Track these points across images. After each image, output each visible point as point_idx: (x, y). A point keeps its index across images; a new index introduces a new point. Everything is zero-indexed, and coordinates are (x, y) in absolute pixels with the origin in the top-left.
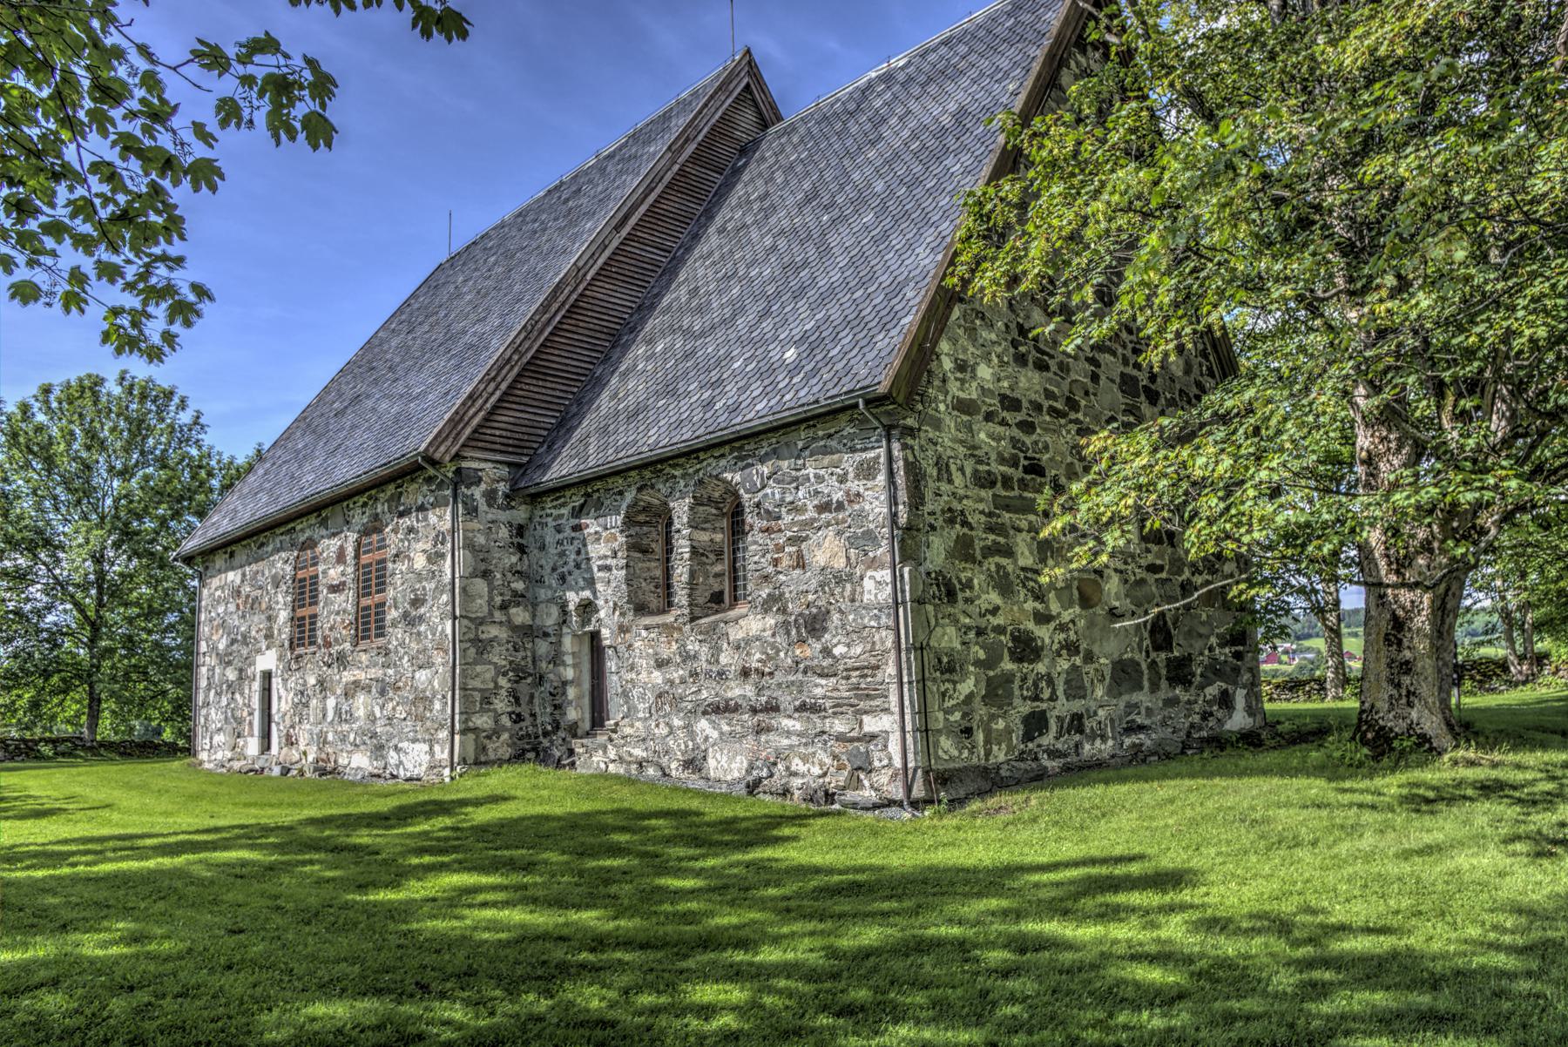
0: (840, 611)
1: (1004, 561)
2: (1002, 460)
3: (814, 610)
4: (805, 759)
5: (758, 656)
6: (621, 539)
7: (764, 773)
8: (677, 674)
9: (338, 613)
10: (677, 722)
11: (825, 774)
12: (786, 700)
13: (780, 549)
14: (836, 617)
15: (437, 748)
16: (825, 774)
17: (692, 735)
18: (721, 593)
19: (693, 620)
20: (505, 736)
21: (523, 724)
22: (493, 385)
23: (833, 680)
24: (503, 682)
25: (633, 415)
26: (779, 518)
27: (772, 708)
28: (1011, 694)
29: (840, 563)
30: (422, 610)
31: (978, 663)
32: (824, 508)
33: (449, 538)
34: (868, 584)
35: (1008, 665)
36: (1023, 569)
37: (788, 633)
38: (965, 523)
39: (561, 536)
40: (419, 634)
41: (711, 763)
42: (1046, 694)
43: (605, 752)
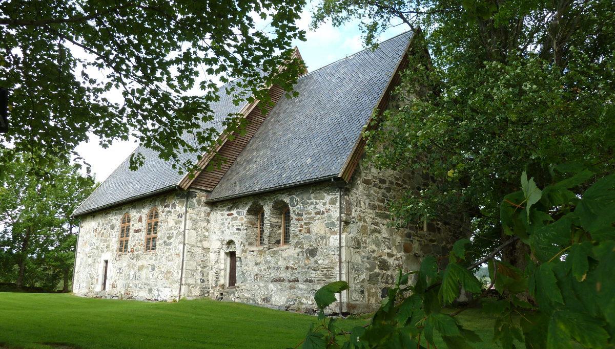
0: (322, 248)
1: (378, 235)
2: (379, 201)
3: (313, 248)
4: (306, 298)
5: (292, 262)
6: (245, 220)
7: (292, 303)
10: (261, 285)
11: (313, 304)
12: (301, 278)
13: (301, 226)
14: (320, 250)
15: (174, 290)
16: (313, 304)
18: (280, 241)
19: (269, 249)
20: (199, 287)
21: (205, 284)
22: (203, 163)
23: (318, 272)
24: (199, 268)
25: (252, 177)
26: (302, 216)
27: (296, 281)
28: (378, 281)
29: (322, 233)
30: (171, 241)
31: (367, 269)
32: (318, 213)
33: (184, 216)
34: (331, 239)
35: (377, 270)
36: (384, 238)
37: (303, 255)
38: (365, 221)
39: (223, 217)
40: (170, 249)
41: (273, 299)
42: (391, 281)
43: (234, 295)
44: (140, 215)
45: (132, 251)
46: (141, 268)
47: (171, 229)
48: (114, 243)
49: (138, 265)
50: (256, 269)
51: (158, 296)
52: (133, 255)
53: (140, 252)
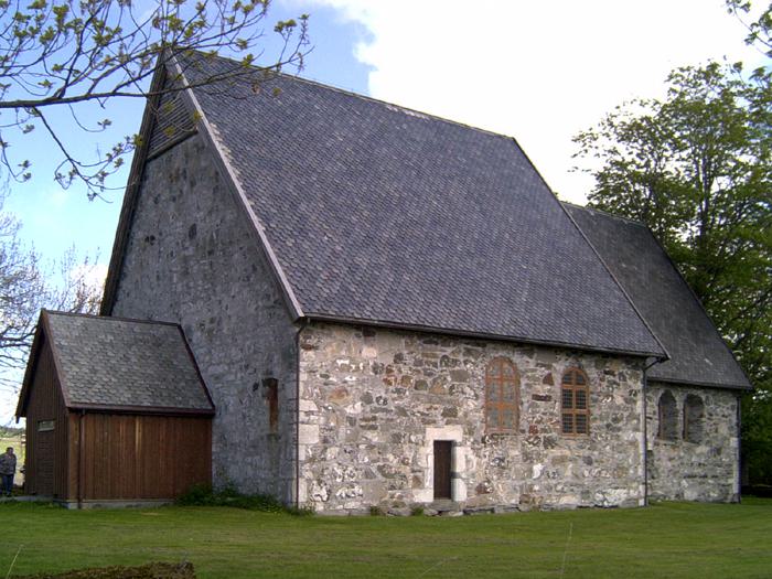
8: (676, 463)
9: (544, 414)
17: (680, 484)
27: (705, 476)
30: (620, 425)
41: (685, 495)
44: (547, 372)
45: (533, 430)
46: (562, 460)
47: (618, 407)
48: (471, 405)
49: (551, 455)
50: (669, 464)
51: (603, 502)
52: (537, 438)
53: (554, 434)
